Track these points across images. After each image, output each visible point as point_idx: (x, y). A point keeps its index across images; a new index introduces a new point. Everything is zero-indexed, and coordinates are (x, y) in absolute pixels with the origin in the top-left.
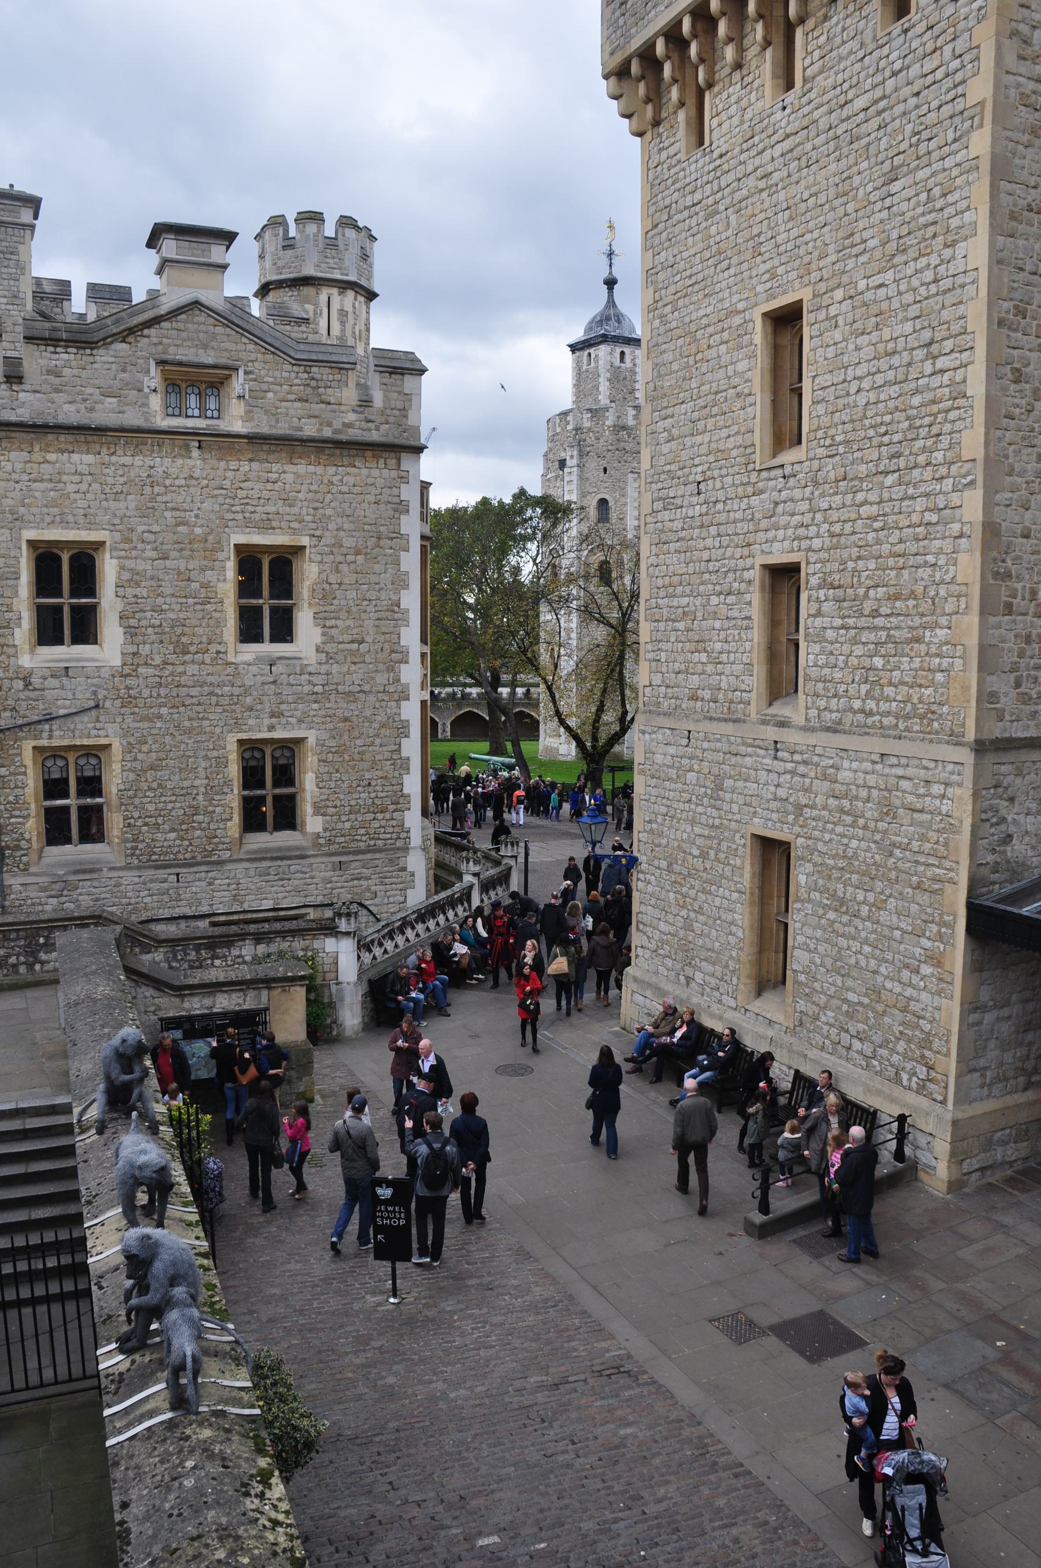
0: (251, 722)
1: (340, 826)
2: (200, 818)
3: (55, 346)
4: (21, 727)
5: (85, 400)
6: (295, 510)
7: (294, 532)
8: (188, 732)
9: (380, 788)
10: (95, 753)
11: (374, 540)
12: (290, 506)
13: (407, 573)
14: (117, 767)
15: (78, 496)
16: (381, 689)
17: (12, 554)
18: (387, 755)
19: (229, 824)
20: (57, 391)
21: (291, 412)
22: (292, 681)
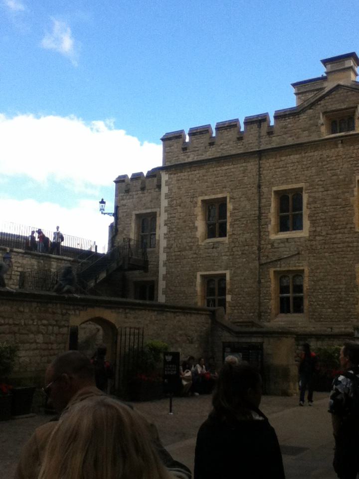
2: (343, 303)
3: (285, 118)
10: (299, 274)
14: (306, 279)
15: (292, 172)
19: (356, 306)
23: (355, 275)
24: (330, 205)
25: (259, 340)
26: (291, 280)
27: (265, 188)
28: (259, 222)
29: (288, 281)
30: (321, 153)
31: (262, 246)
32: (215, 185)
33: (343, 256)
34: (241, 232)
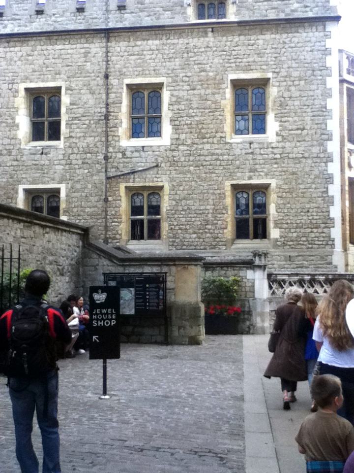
0: (239, 174)
1: (290, 235)
2: (209, 227)
4: (119, 176)
5: (155, 14)
6: (265, 59)
7: (264, 71)
8: (205, 180)
9: (315, 214)
10: (156, 191)
11: (310, 72)
12: (261, 57)
13: (330, 89)
14: (166, 198)
15: (151, 61)
16: (315, 155)
17: (119, 91)
18: (320, 194)
19: (225, 231)
20: (141, 11)
21: (262, 7)
22: (262, 152)
23: (224, 194)
24: (197, 108)
25: (155, 270)
26: (145, 198)
27: (114, 79)
28: (107, 123)
29: (143, 201)
30: (187, 41)
31: (109, 155)
32: (44, 69)
33: (211, 171)
34: (82, 134)
